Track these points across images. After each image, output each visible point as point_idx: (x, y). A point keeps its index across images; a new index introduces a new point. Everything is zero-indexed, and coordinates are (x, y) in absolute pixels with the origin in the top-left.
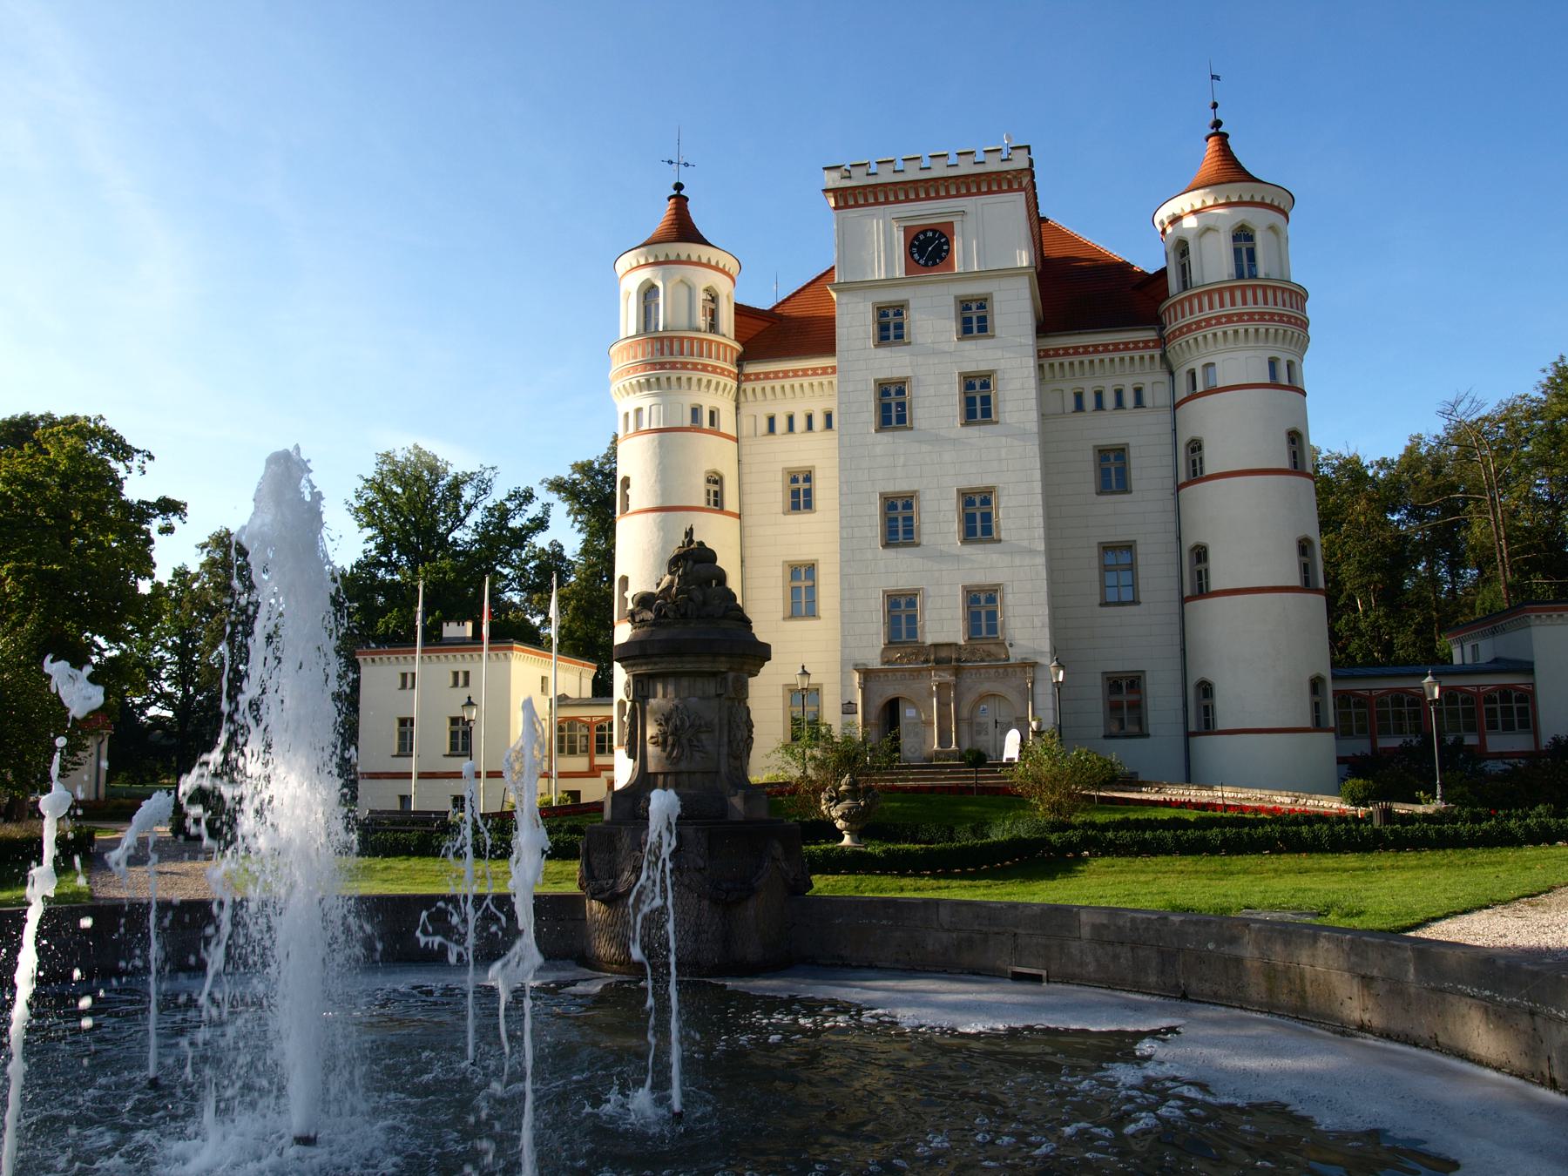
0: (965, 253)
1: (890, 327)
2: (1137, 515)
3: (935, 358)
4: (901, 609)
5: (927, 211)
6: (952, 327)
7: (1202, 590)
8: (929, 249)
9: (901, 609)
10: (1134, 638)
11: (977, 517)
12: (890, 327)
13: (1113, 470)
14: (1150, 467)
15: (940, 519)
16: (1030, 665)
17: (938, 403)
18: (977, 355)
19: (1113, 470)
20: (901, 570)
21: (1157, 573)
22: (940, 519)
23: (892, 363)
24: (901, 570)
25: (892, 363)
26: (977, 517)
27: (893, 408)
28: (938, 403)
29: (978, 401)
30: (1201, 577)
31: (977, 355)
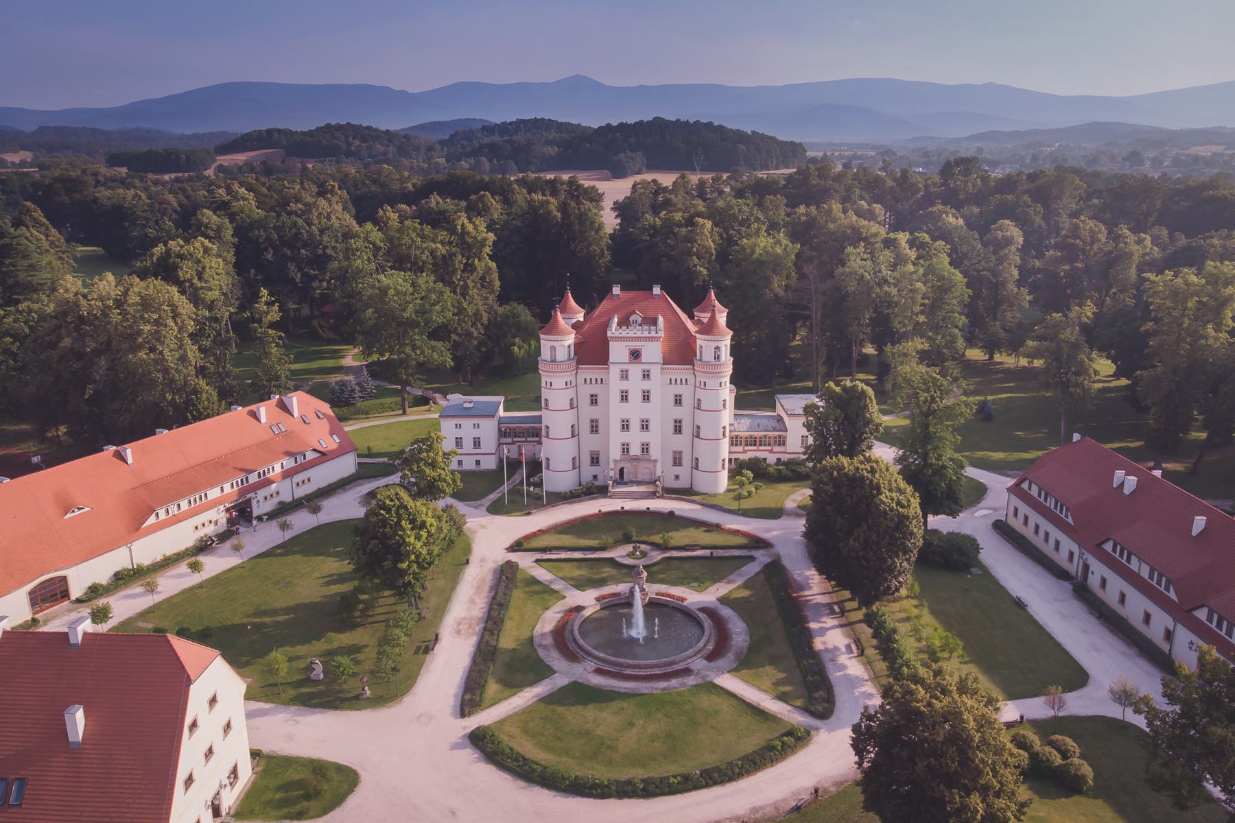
0: (644, 358)
1: (625, 375)
2: (683, 413)
3: (635, 385)
4: (626, 449)
5: (635, 345)
6: (640, 376)
7: (698, 437)
8: (635, 355)
9: (626, 449)
10: (681, 442)
11: (645, 426)
12: (625, 375)
13: (678, 401)
14: (687, 401)
15: (635, 425)
16: (655, 461)
17: (635, 396)
18: (646, 385)
19: (678, 401)
20: (625, 437)
21: (687, 428)
22: (635, 425)
23: (624, 385)
24: (625, 437)
25: (624, 385)
26: (645, 426)
27: (624, 397)
28: (635, 396)
29: (646, 397)
30: (698, 433)
31: (646, 385)
